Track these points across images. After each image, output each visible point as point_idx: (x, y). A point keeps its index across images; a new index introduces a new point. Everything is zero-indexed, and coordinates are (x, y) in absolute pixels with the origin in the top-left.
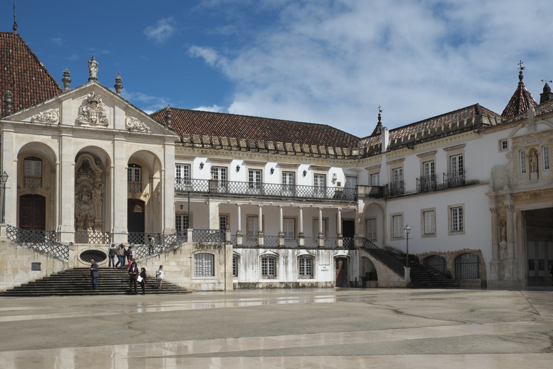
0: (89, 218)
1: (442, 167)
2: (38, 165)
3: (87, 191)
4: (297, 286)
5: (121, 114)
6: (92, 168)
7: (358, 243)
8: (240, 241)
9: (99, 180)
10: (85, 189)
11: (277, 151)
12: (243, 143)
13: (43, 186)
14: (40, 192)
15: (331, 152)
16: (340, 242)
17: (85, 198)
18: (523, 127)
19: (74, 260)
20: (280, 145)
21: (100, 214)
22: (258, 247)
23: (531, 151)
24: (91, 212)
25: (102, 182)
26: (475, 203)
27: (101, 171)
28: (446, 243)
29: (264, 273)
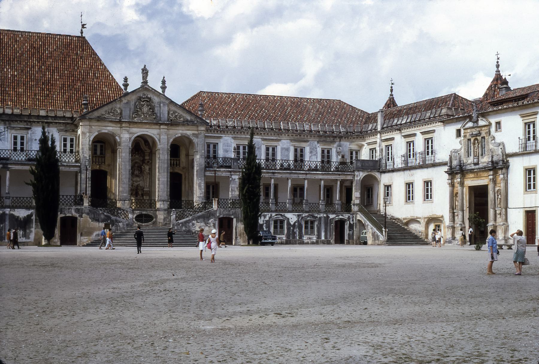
0: (139, 188)
3: (138, 167)
6: (142, 148)
7: (355, 208)
9: (147, 158)
10: (136, 165)
13: (106, 163)
14: (103, 168)
17: (137, 172)
18: (470, 121)
21: (148, 185)
23: (475, 140)
24: (141, 183)
25: (149, 159)
26: (440, 178)
27: (148, 151)
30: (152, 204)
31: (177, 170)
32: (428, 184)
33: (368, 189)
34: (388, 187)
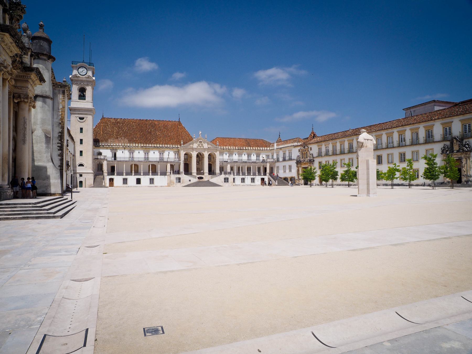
1: (287, 155)
2: (188, 157)
4: (250, 185)
5: (206, 144)
7: (268, 174)
8: (235, 174)
11: (246, 150)
12: (237, 148)
14: (187, 162)
15: (261, 149)
16: (262, 174)
19: (197, 180)
20: (247, 148)
22: (240, 175)
28: (288, 175)
29: (242, 182)
30: (204, 174)
31: (210, 163)
32: (290, 167)
33: (272, 169)
34: (278, 167)
